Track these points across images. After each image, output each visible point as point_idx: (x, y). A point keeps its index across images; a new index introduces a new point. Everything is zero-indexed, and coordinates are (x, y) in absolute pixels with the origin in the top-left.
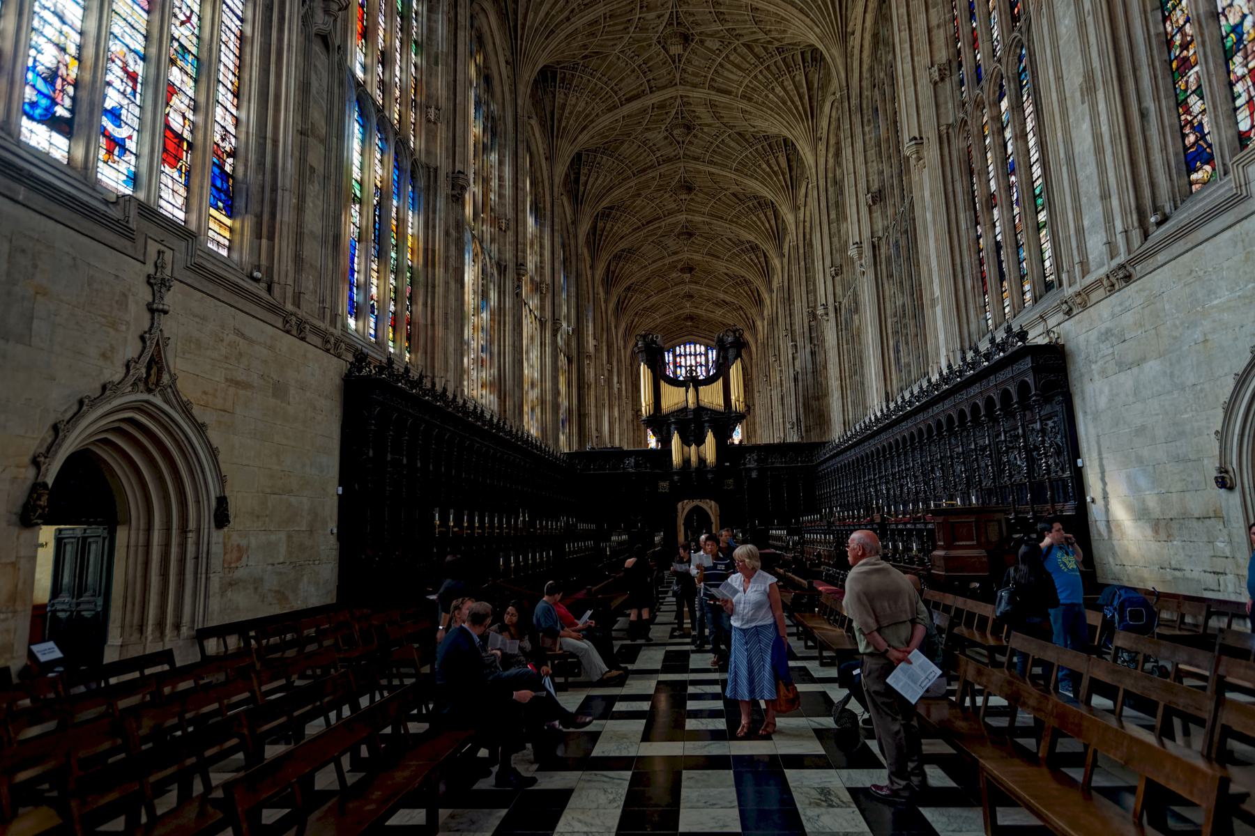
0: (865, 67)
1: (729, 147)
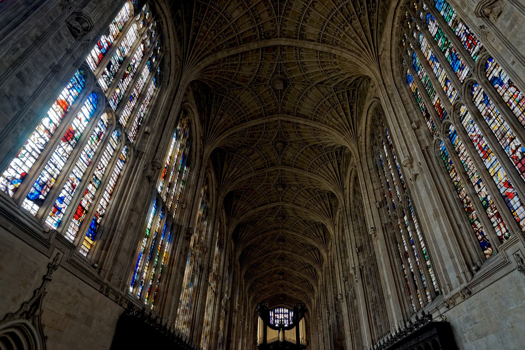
0: (351, 200)
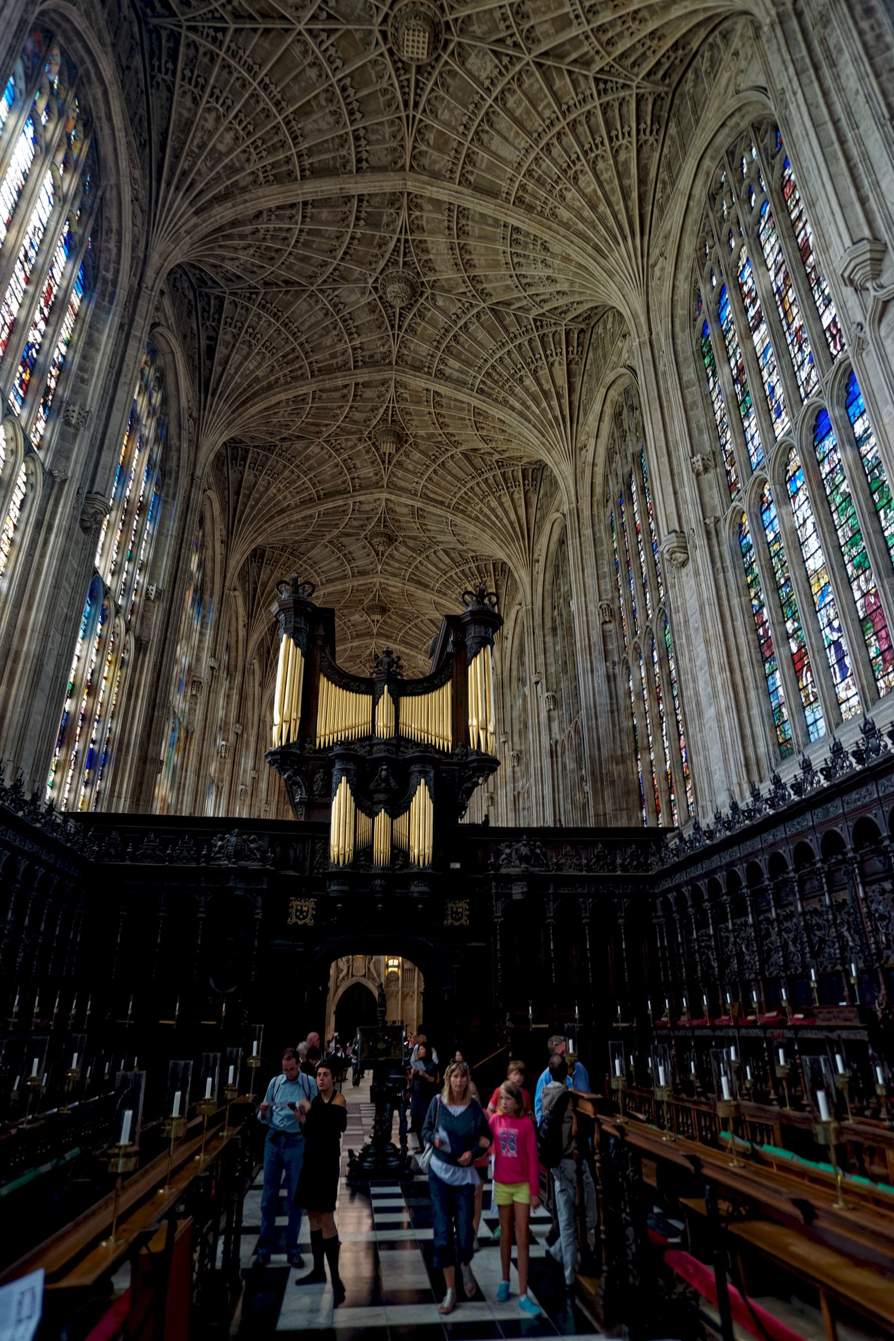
1: (475, 340)
